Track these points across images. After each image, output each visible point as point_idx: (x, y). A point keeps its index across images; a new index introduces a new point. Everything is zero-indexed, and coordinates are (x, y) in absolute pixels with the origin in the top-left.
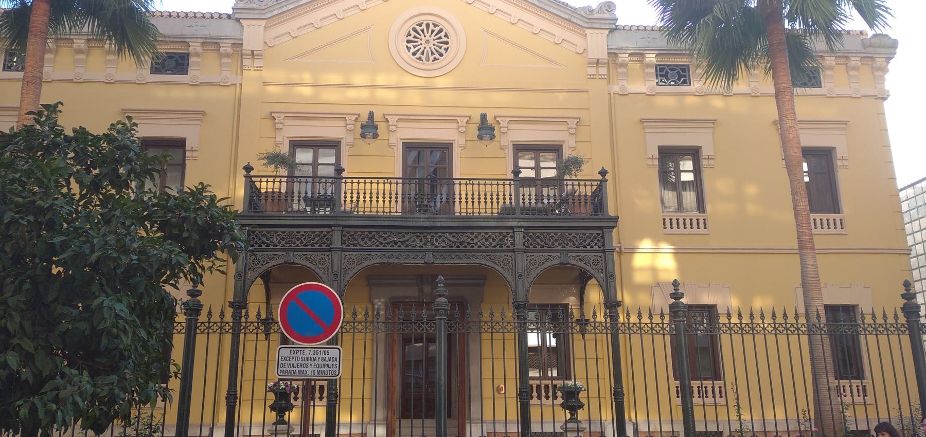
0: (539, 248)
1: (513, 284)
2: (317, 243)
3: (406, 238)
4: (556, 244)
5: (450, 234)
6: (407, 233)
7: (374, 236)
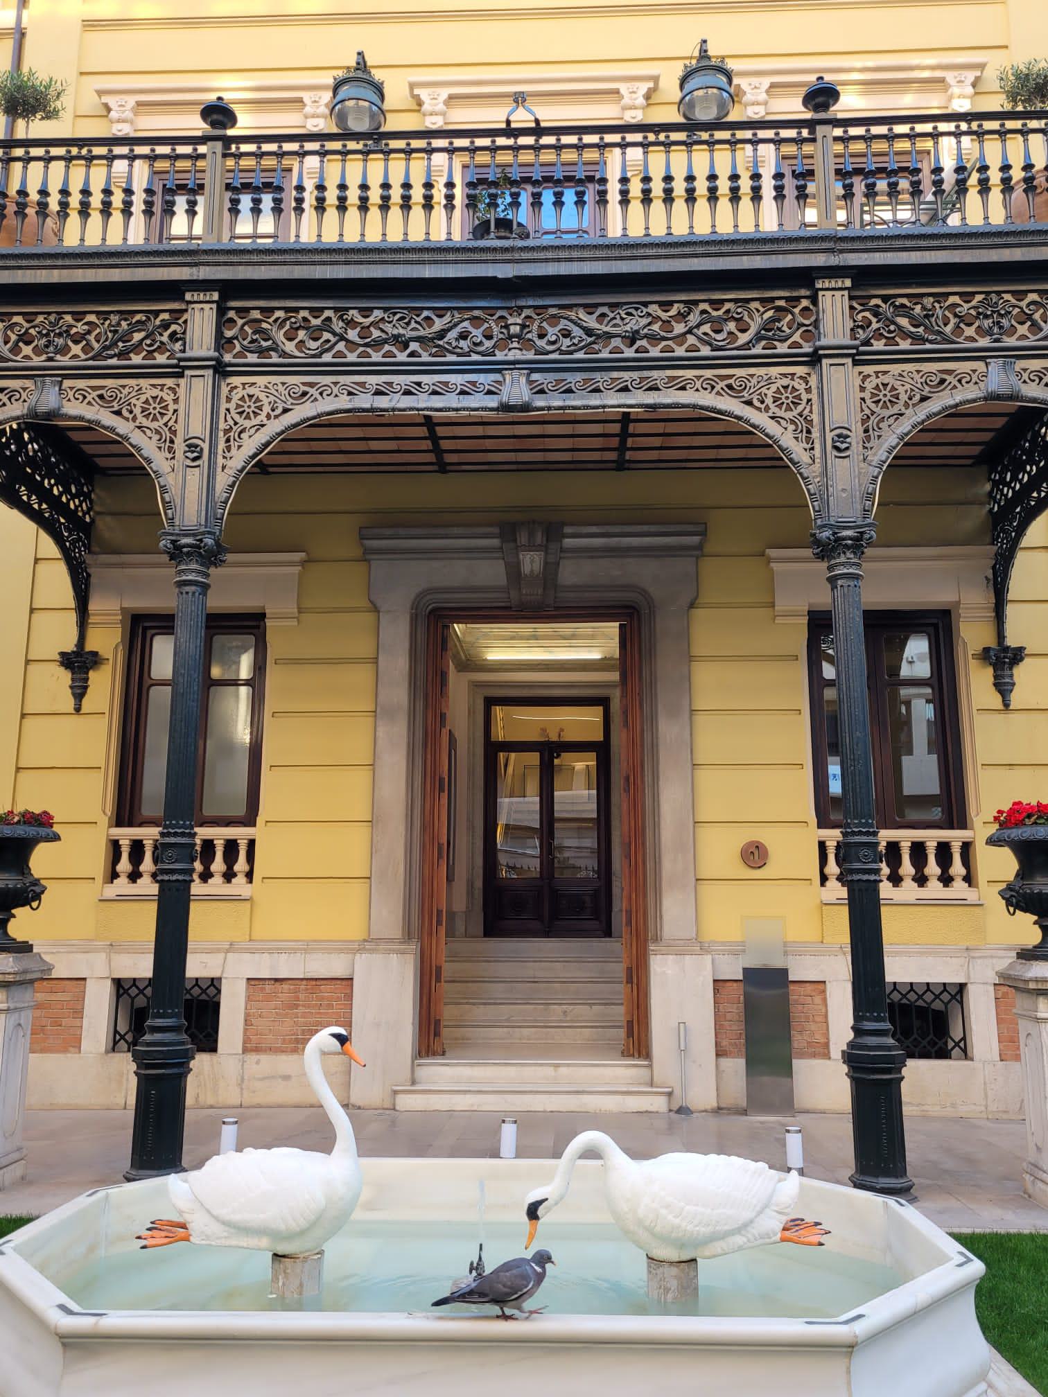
0: (905, 345)
1: (813, 472)
2: (137, 348)
3: (439, 324)
4: (970, 331)
5: (590, 309)
6: (441, 313)
7: (327, 325)
